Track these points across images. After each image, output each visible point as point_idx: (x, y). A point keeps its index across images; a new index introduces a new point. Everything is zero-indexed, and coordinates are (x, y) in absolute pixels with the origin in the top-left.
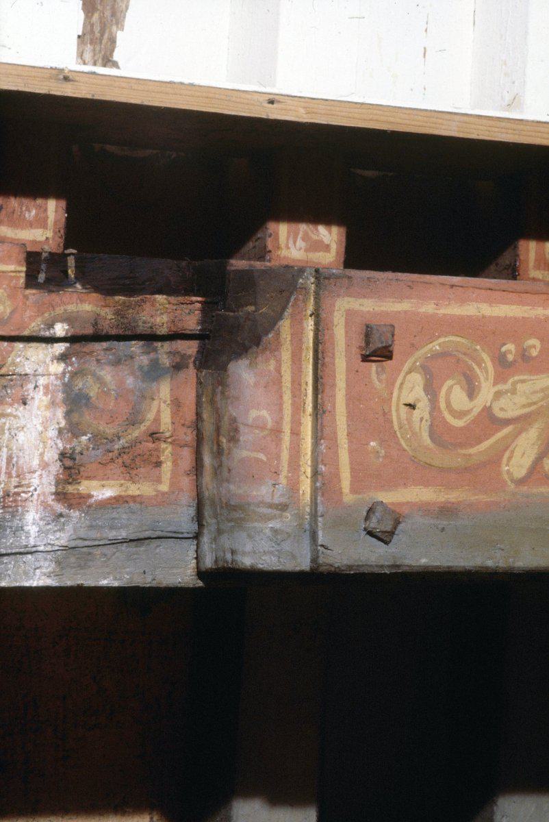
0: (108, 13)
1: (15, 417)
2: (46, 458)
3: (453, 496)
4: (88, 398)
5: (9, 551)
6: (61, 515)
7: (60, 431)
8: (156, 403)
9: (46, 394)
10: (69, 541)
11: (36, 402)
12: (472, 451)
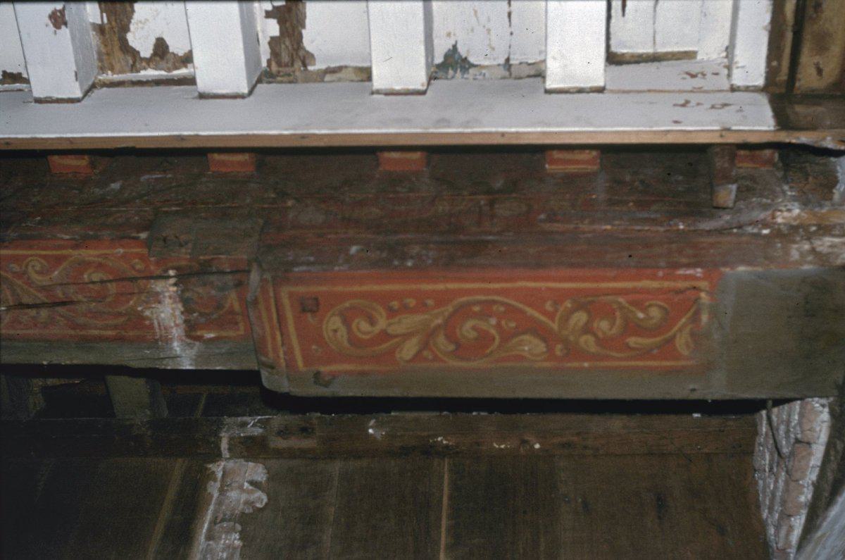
3: (366, 368)
7: (182, 313)
11: (166, 302)
12: (376, 348)
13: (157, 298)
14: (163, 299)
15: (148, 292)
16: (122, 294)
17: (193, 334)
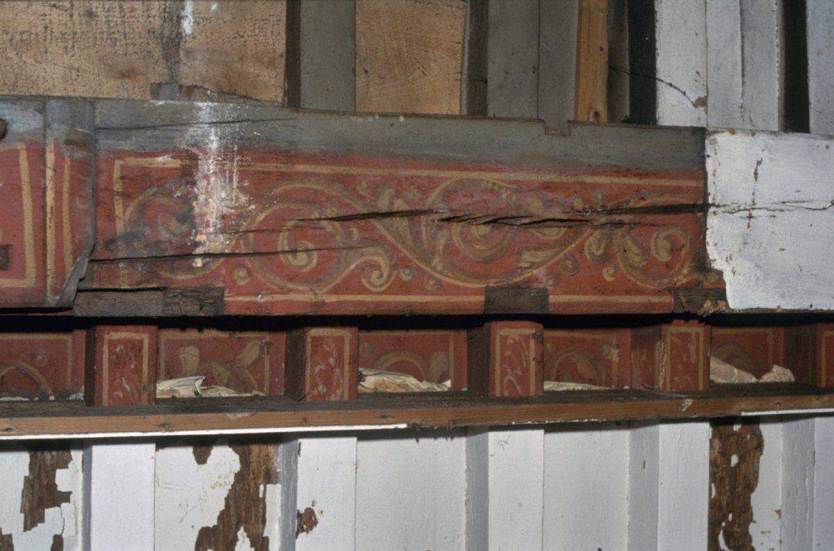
0: (37, 486)
1: (228, 207)
2: (205, 181)
4: (178, 220)
5: (228, 125)
6: (193, 146)
7: (196, 198)
8: (127, 218)
9: (208, 221)
10: (187, 130)
11: (214, 216)
13: (228, 224)
14: (218, 221)
15: (237, 232)
16: (273, 231)
17: (187, 162)
